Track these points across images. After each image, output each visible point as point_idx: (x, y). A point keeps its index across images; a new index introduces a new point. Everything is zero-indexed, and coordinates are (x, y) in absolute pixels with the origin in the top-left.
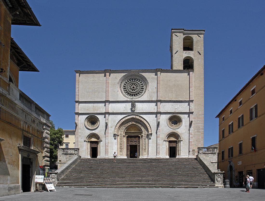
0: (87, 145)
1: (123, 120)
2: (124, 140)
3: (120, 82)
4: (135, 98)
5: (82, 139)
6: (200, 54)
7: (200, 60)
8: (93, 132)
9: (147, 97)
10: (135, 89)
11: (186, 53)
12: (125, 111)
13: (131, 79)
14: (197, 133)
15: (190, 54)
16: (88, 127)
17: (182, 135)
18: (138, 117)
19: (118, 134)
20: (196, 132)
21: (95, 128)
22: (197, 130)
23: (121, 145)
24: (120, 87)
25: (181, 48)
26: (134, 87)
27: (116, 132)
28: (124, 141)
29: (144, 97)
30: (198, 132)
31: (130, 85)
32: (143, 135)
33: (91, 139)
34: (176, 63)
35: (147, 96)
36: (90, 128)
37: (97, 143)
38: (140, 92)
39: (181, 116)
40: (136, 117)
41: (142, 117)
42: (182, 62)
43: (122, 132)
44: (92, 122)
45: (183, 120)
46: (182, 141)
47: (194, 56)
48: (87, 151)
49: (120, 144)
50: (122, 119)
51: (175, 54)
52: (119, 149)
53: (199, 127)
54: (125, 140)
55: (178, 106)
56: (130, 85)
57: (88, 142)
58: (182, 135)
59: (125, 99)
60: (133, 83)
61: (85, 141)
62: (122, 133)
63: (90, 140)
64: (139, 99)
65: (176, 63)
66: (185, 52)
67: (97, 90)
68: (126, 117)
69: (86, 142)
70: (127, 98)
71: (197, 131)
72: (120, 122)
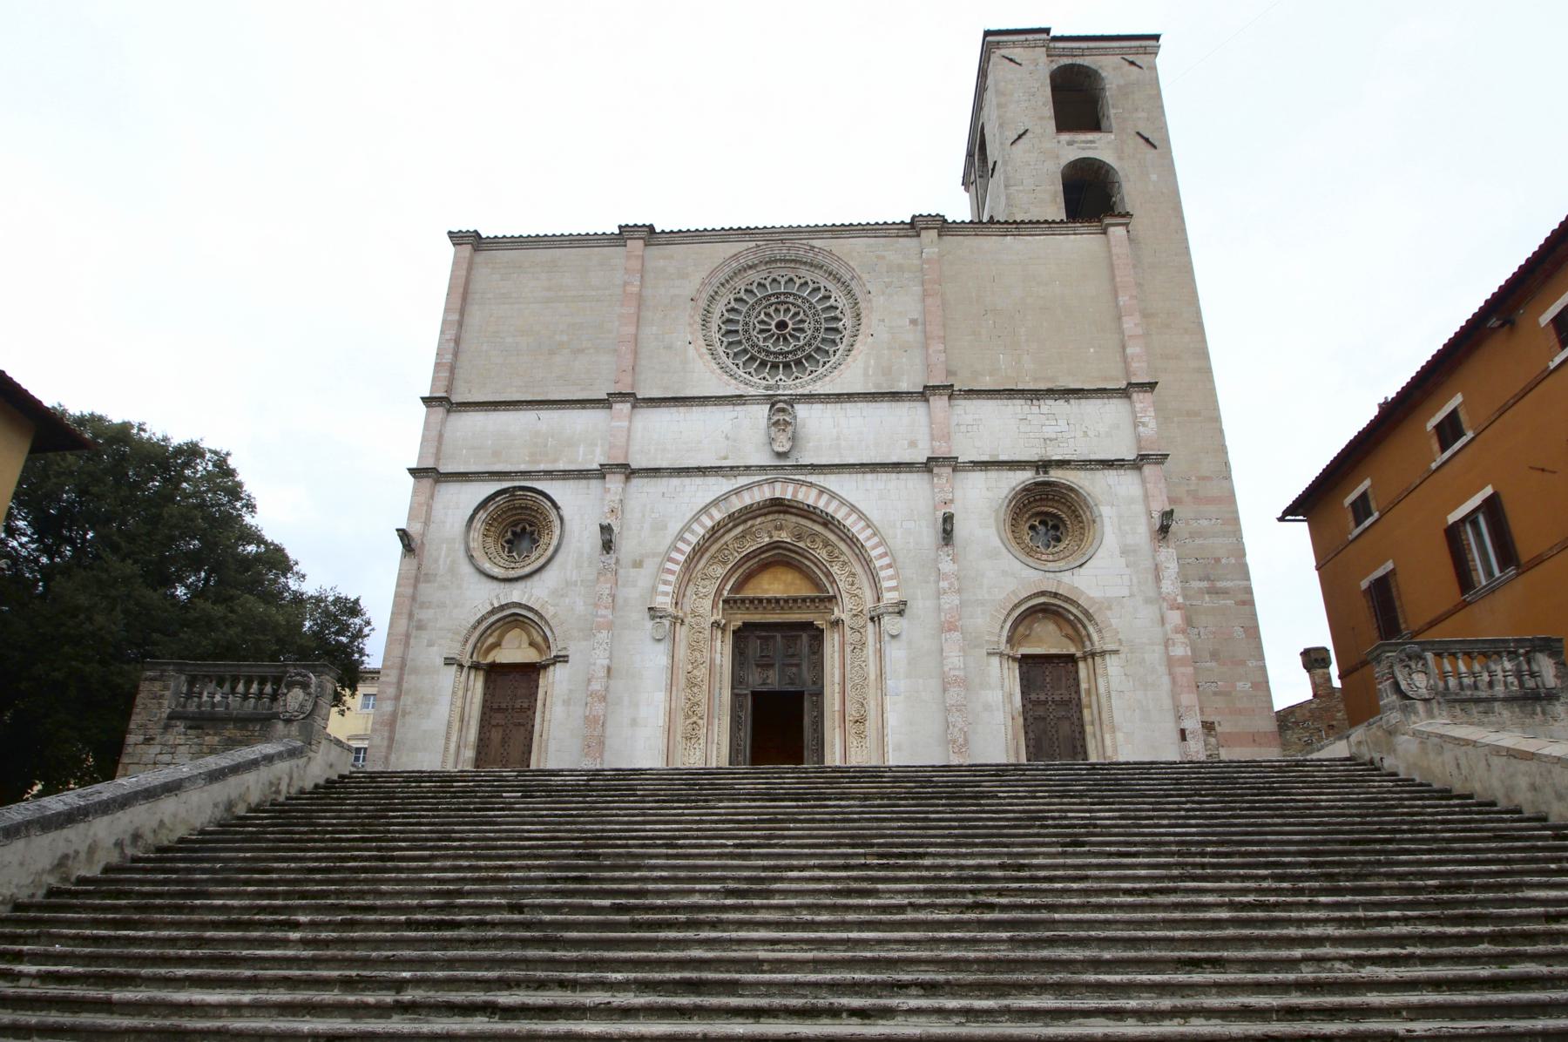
0: (460, 693)
1: (712, 518)
2: (718, 656)
3: (705, 296)
4: (788, 385)
5: (435, 648)
6: (1155, 147)
7: (1154, 177)
8: (516, 594)
9: (866, 374)
10: (791, 335)
11: (1070, 143)
12: (725, 458)
13: (769, 280)
14: (1207, 597)
15: (1096, 148)
16: (487, 566)
17: (1109, 613)
18: (808, 497)
19: (681, 614)
20: (1201, 591)
21: (528, 570)
22: (1207, 578)
23: (695, 690)
24: (705, 323)
25: (1041, 118)
26: (782, 325)
27: (666, 594)
28: (718, 662)
29: (851, 373)
30: (1214, 591)
31: (762, 316)
32: (843, 617)
33: (497, 645)
34: (1021, 188)
35: (866, 369)
36: (496, 571)
37: (530, 673)
38: (818, 349)
39: (1086, 482)
40: (795, 493)
41: (833, 496)
42: (1053, 184)
43: (704, 605)
44: (514, 533)
45: (1107, 513)
46: (1116, 652)
47: (1120, 158)
48: (454, 738)
49: (692, 684)
50: (705, 510)
51: (1012, 143)
52: (680, 726)
53: (1218, 560)
54: (722, 652)
55: (1062, 423)
56: (762, 316)
57: (476, 667)
58: (1109, 613)
59: (732, 389)
60: (778, 303)
61: (449, 662)
62: (708, 603)
63: (489, 659)
64: (820, 388)
65: (1021, 188)
66: (1065, 137)
67: (565, 338)
68: (737, 492)
69: (461, 666)
70: (742, 386)
71: (1205, 584)
72: (693, 532)
